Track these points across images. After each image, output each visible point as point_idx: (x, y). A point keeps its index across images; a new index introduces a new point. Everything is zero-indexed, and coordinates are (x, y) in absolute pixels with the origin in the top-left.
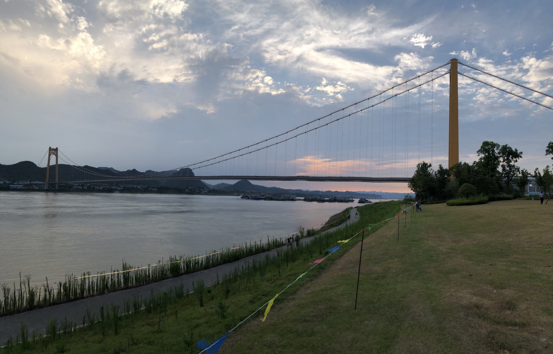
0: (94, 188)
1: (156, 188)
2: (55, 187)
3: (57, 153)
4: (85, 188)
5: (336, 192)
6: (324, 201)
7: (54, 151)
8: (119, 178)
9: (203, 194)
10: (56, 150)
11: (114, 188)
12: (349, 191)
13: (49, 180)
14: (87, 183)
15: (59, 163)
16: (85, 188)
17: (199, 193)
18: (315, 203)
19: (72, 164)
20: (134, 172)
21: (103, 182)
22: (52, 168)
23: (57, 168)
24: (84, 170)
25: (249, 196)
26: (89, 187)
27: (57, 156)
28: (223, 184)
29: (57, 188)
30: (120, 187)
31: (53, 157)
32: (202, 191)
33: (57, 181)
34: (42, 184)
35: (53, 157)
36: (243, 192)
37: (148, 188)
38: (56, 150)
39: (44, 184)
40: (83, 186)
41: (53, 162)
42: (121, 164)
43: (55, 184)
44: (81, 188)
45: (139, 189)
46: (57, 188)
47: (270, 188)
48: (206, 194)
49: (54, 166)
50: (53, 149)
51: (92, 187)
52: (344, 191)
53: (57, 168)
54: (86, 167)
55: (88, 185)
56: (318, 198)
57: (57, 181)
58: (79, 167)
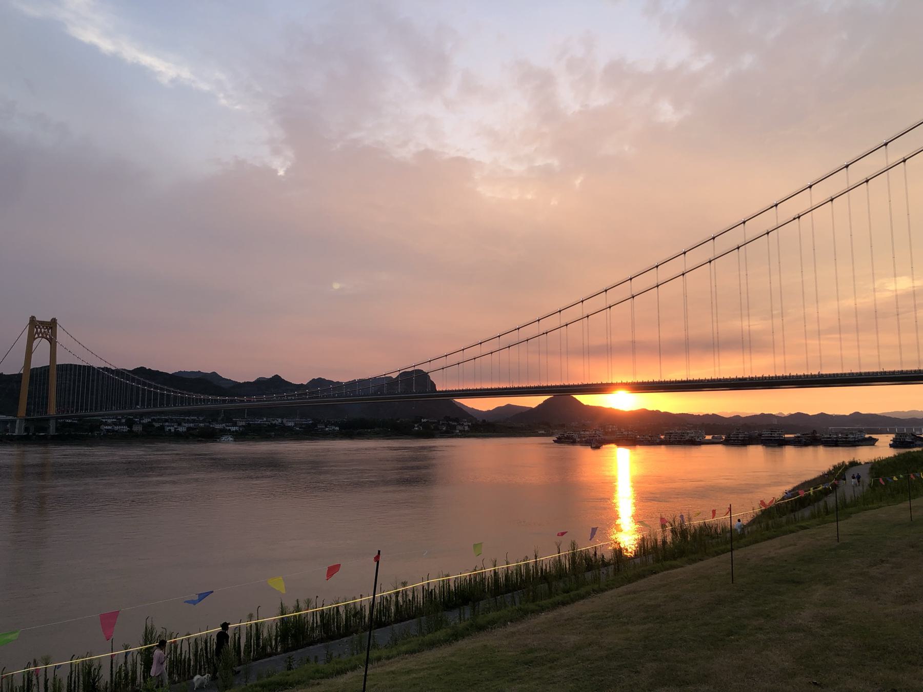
0: (162, 428)
1: (335, 424)
2: (45, 429)
3: (54, 334)
4: (137, 428)
5: (822, 416)
6: (782, 443)
7: (43, 329)
8: (232, 401)
9: (457, 436)
10: (52, 325)
11: (218, 426)
12: (864, 411)
13: (28, 412)
14: (142, 415)
15: (60, 361)
16: (137, 428)
17: (450, 433)
18: (756, 452)
19: (97, 364)
20: (276, 383)
21: (189, 413)
22: (39, 376)
23: (53, 374)
24: (133, 380)
25: (575, 436)
26: (150, 425)
27: (53, 342)
28: (509, 406)
29: (52, 431)
30: (235, 424)
31: (42, 347)
32: (454, 427)
33: (52, 410)
34: (6, 422)
35: (42, 347)
36: (563, 426)
37: (314, 425)
38: (52, 325)
39: (14, 422)
40: (130, 423)
41: (40, 359)
42: (240, 360)
43: (48, 420)
44: (125, 429)
45: (290, 429)
46: (52, 431)
47: (631, 412)
48: (464, 435)
49: (45, 370)
50: (42, 323)
51: (157, 425)
52: (847, 411)
53: (53, 374)
54: (141, 371)
55: (146, 421)
56: (766, 433)
57: (52, 410)
58: (120, 373)
